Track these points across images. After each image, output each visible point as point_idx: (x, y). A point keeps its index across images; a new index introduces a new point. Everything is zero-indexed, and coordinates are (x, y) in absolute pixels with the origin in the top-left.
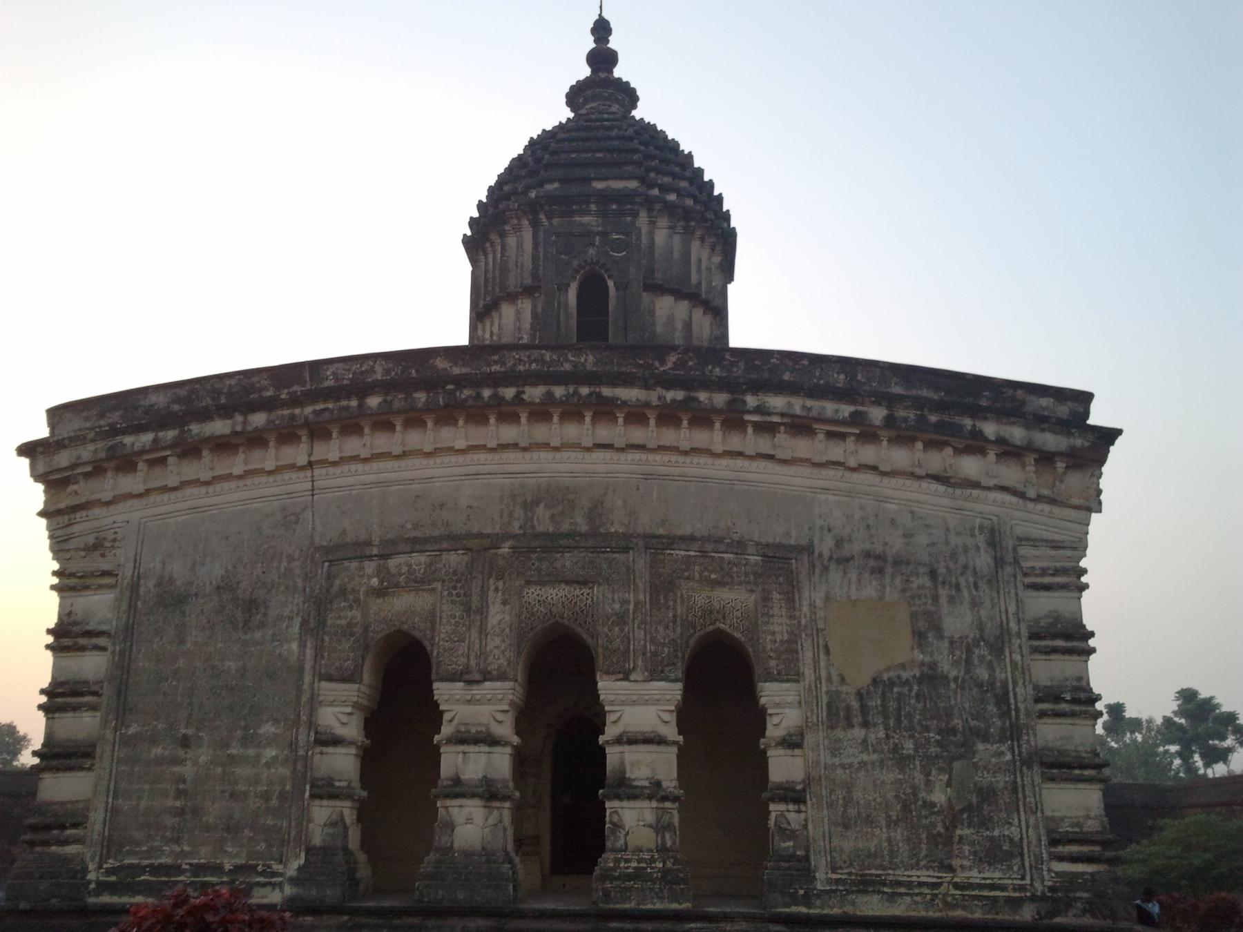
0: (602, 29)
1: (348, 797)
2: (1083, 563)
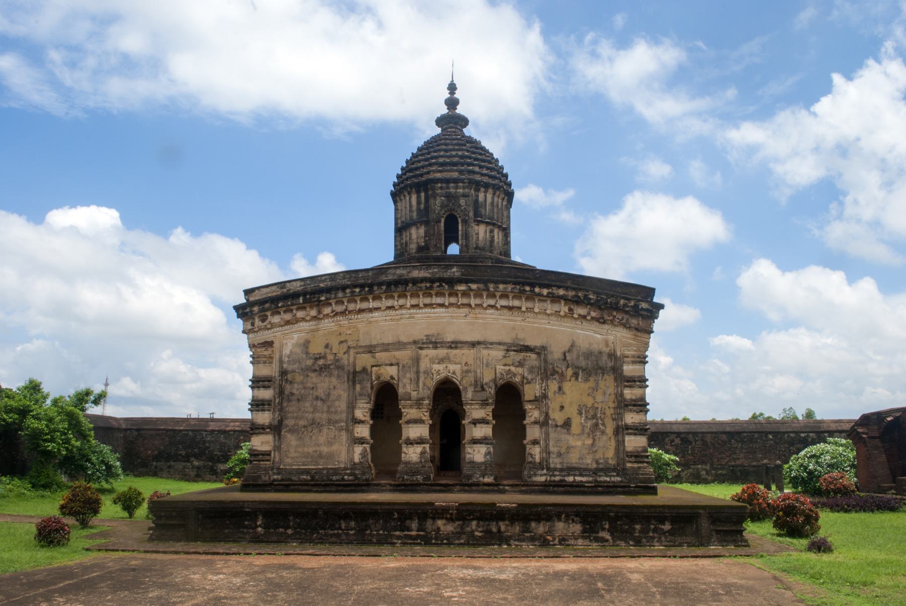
0: (452, 88)
2: (647, 353)
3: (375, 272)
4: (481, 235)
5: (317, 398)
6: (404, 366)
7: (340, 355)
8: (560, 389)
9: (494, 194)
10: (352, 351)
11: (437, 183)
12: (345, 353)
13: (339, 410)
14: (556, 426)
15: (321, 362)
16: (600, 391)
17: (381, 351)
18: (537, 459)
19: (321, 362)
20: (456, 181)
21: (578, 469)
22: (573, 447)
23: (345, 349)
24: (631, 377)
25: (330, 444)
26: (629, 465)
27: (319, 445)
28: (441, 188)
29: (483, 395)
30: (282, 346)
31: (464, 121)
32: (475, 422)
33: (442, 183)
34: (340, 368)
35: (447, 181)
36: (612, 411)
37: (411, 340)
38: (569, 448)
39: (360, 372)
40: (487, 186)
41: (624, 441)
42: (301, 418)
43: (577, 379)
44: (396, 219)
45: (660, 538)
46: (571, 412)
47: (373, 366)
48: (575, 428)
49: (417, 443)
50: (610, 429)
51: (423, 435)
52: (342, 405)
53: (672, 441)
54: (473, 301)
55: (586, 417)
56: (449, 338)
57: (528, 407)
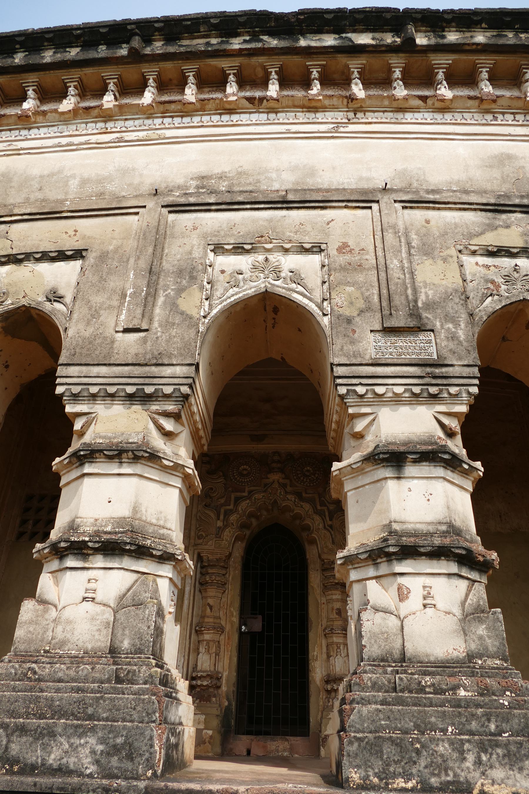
32: (394, 458)
37: (146, 188)
56: (280, 182)
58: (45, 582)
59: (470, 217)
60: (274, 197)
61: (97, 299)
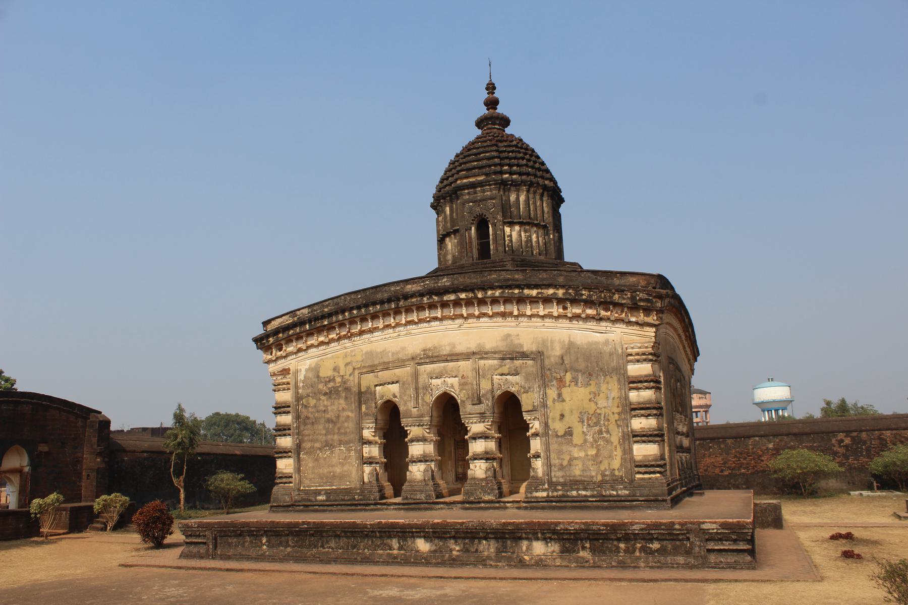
0: (491, 88)
1: (377, 463)
3: (371, 291)
4: (515, 235)
5: (329, 421)
6: (404, 383)
7: (347, 377)
8: (560, 395)
9: (528, 191)
10: (357, 372)
11: (464, 189)
12: (350, 375)
13: (348, 430)
14: (557, 436)
15: (331, 385)
16: (601, 395)
17: (383, 370)
18: (540, 472)
19: (331, 385)
20: (481, 184)
21: (581, 482)
22: (576, 458)
23: (351, 371)
24: (636, 377)
25: (342, 464)
26: (638, 476)
27: (333, 466)
28: (469, 194)
29: (481, 408)
30: (297, 371)
31: (505, 122)
32: (474, 438)
33: (468, 189)
34: (347, 389)
35: (473, 186)
36: (617, 416)
37: (410, 357)
38: (571, 459)
39: (366, 392)
40: (517, 185)
41: (631, 450)
42: (317, 440)
43: (576, 384)
44: (438, 231)
45: (647, 558)
46: (572, 420)
47: (376, 386)
48: (577, 439)
49: (420, 461)
50: (616, 436)
51: (427, 452)
52: (350, 426)
53: (842, 441)
54: (464, 311)
55: (589, 425)
56: (446, 350)
57: (526, 417)
58: (410, 467)
59: (496, 362)
60: (444, 358)
61: (405, 398)
